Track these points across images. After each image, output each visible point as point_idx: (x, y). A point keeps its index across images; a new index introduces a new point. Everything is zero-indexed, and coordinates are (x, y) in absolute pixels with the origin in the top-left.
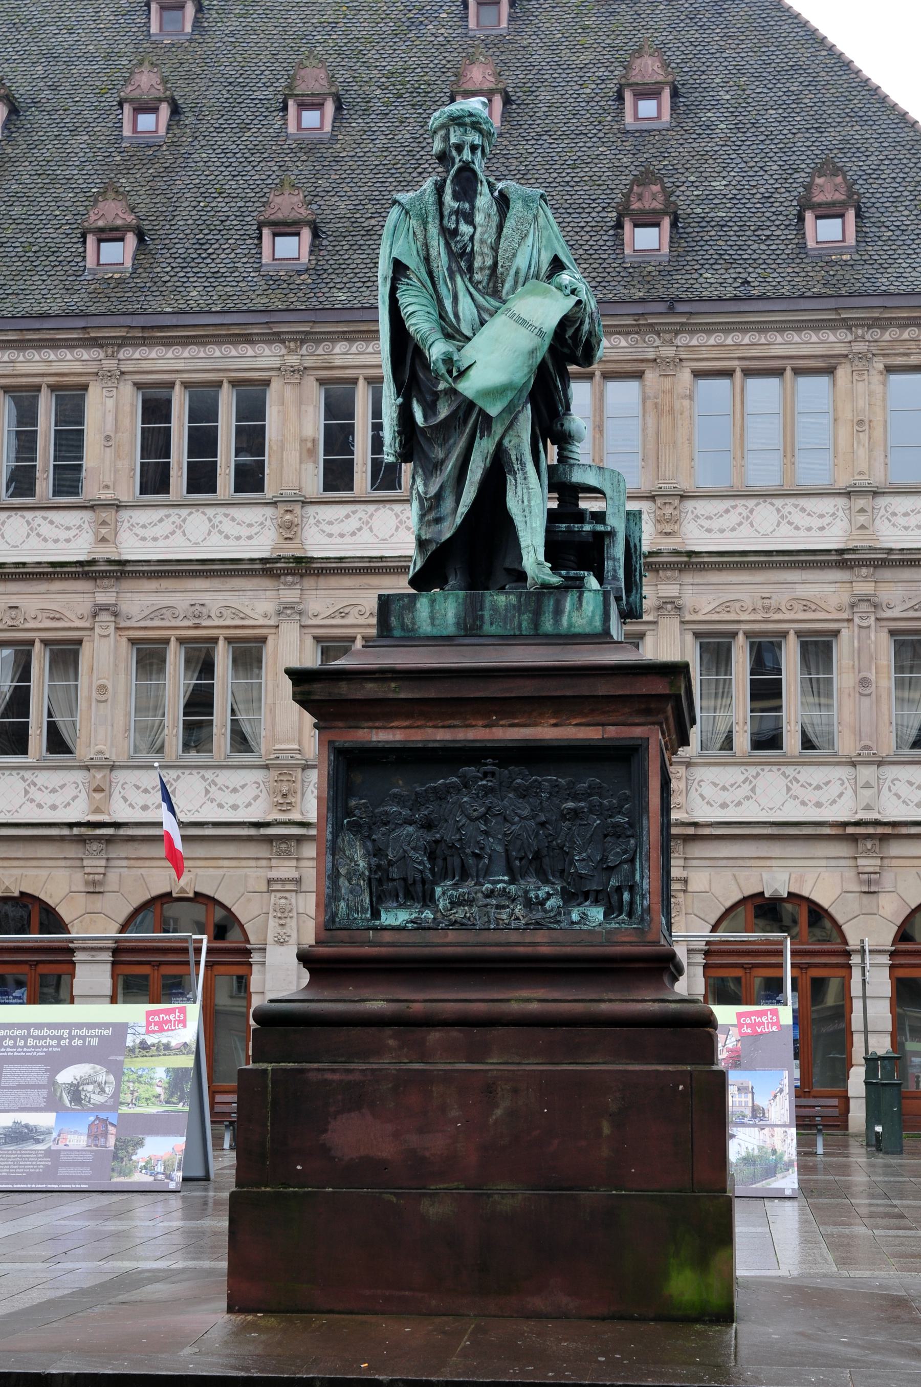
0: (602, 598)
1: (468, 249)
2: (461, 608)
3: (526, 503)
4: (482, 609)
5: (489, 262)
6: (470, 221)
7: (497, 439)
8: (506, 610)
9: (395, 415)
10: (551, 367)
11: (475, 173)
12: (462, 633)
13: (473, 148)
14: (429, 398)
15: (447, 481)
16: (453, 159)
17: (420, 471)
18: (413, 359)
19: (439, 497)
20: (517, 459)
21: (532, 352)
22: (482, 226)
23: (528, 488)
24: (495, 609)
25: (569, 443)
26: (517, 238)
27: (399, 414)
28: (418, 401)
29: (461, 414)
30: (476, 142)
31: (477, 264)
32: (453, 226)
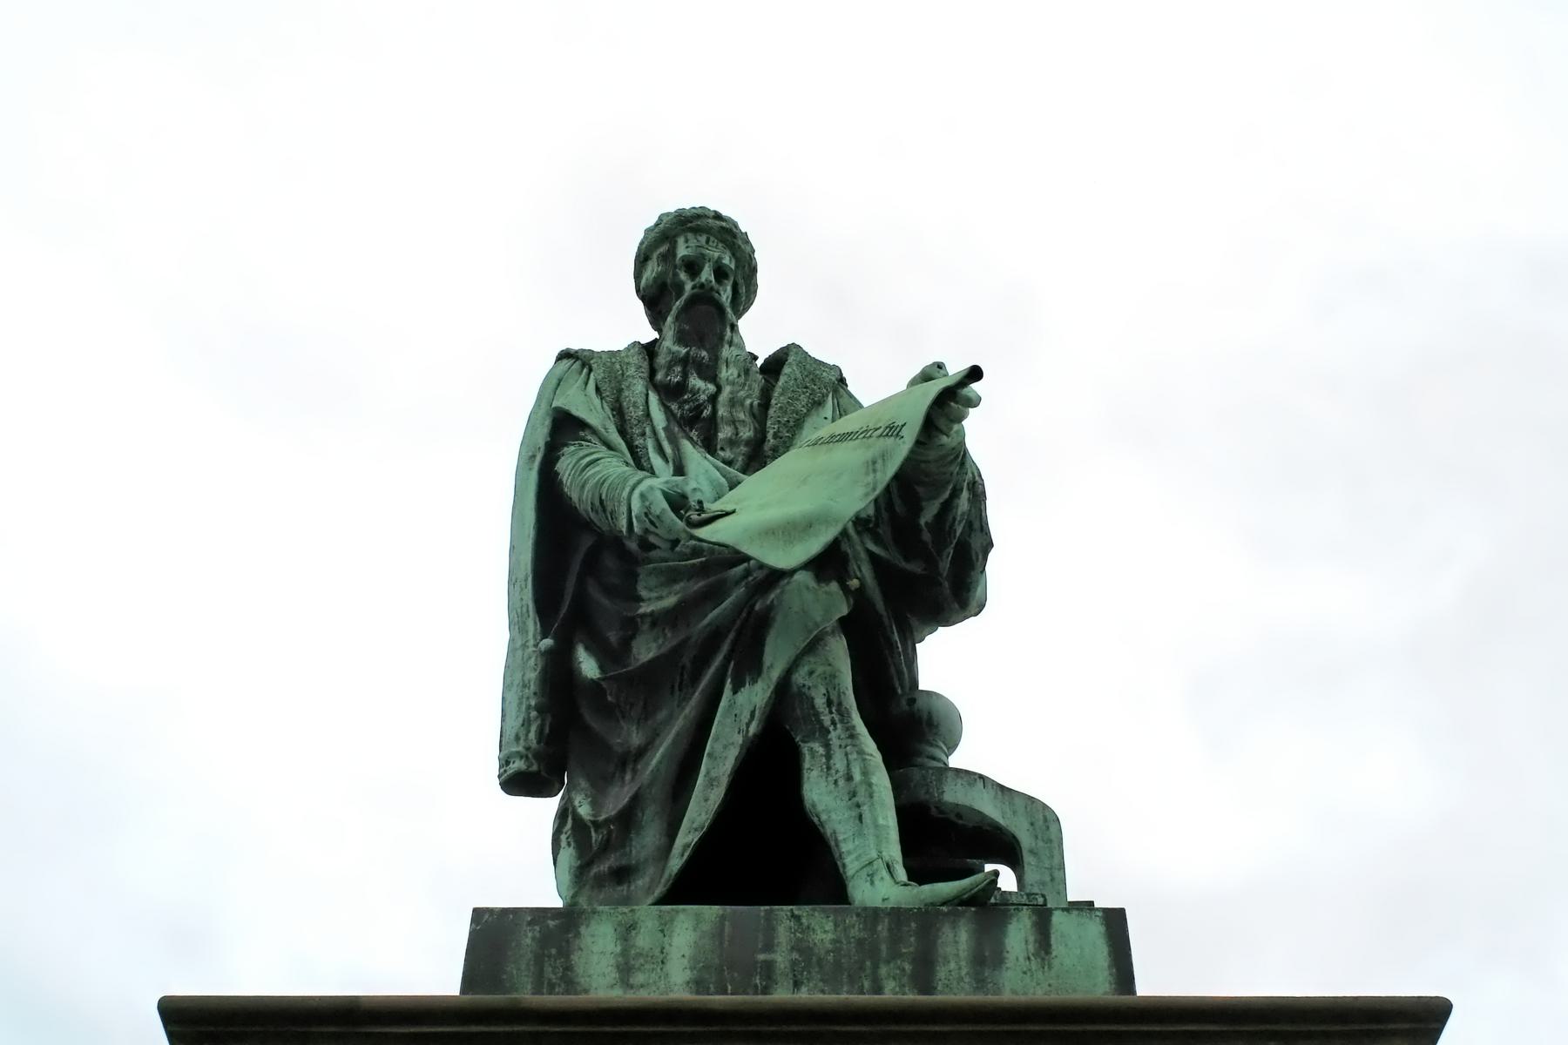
0: (1102, 929)
1: (706, 413)
3: (857, 777)
4: (769, 947)
5: (747, 433)
6: (712, 378)
7: (776, 674)
8: (837, 951)
9: (532, 675)
10: (880, 606)
11: (720, 309)
13: (721, 273)
14: (613, 637)
15: (651, 784)
16: (679, 288)
17: (583, 784)
18: (581, 582)
19: (627, 820)
20: (829, 703)
22: (733, 384)
23: (861, 752)
24: (802, 949)
26: (804, 399)
28: (587, 649)
29: (686, 661)
30: (726, 261)
31: (725, 433)
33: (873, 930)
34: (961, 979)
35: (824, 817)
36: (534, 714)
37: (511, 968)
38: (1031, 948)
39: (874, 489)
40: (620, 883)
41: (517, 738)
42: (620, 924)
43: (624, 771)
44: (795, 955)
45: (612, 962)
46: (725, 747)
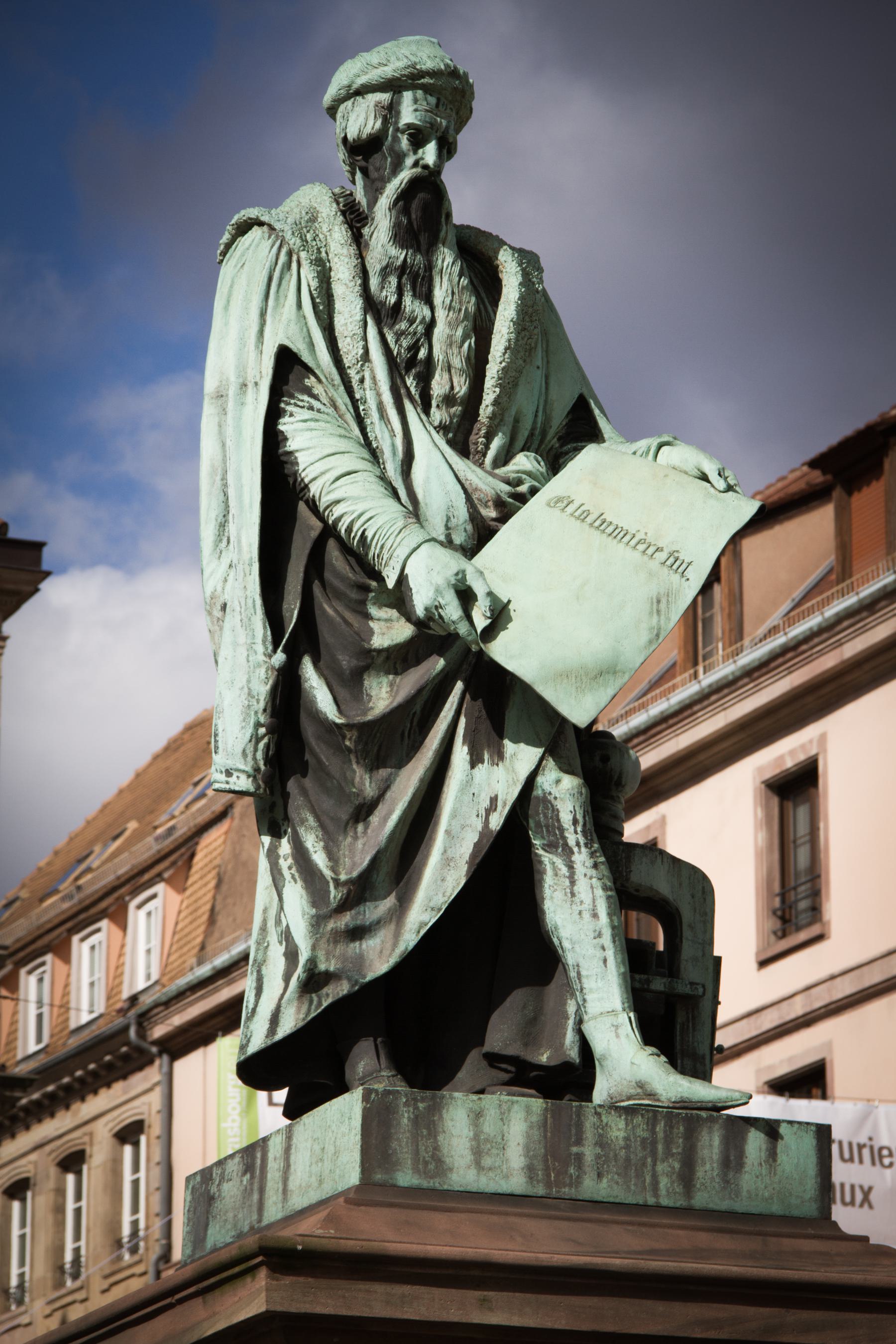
1: (422, 354)
2: (536, 1134)
4: (579, 1141)
5: (462, 388)
7: (523, 770)
8: (627, 1147)
12: (540, 1190)
21: (658, 603)
24: (602, 1142)
25: (612, 798)
29: (418, 708)
31: (439, 386)
32: (393, 299)
33: (653, 1132)
34: (713, 1178)
35: (566, 944)
37: (394, 1145)
38: (763, 1154)
39: (658, 635)
42: (471, 1110)
44: (598, 1150)
45: (468, 1145)
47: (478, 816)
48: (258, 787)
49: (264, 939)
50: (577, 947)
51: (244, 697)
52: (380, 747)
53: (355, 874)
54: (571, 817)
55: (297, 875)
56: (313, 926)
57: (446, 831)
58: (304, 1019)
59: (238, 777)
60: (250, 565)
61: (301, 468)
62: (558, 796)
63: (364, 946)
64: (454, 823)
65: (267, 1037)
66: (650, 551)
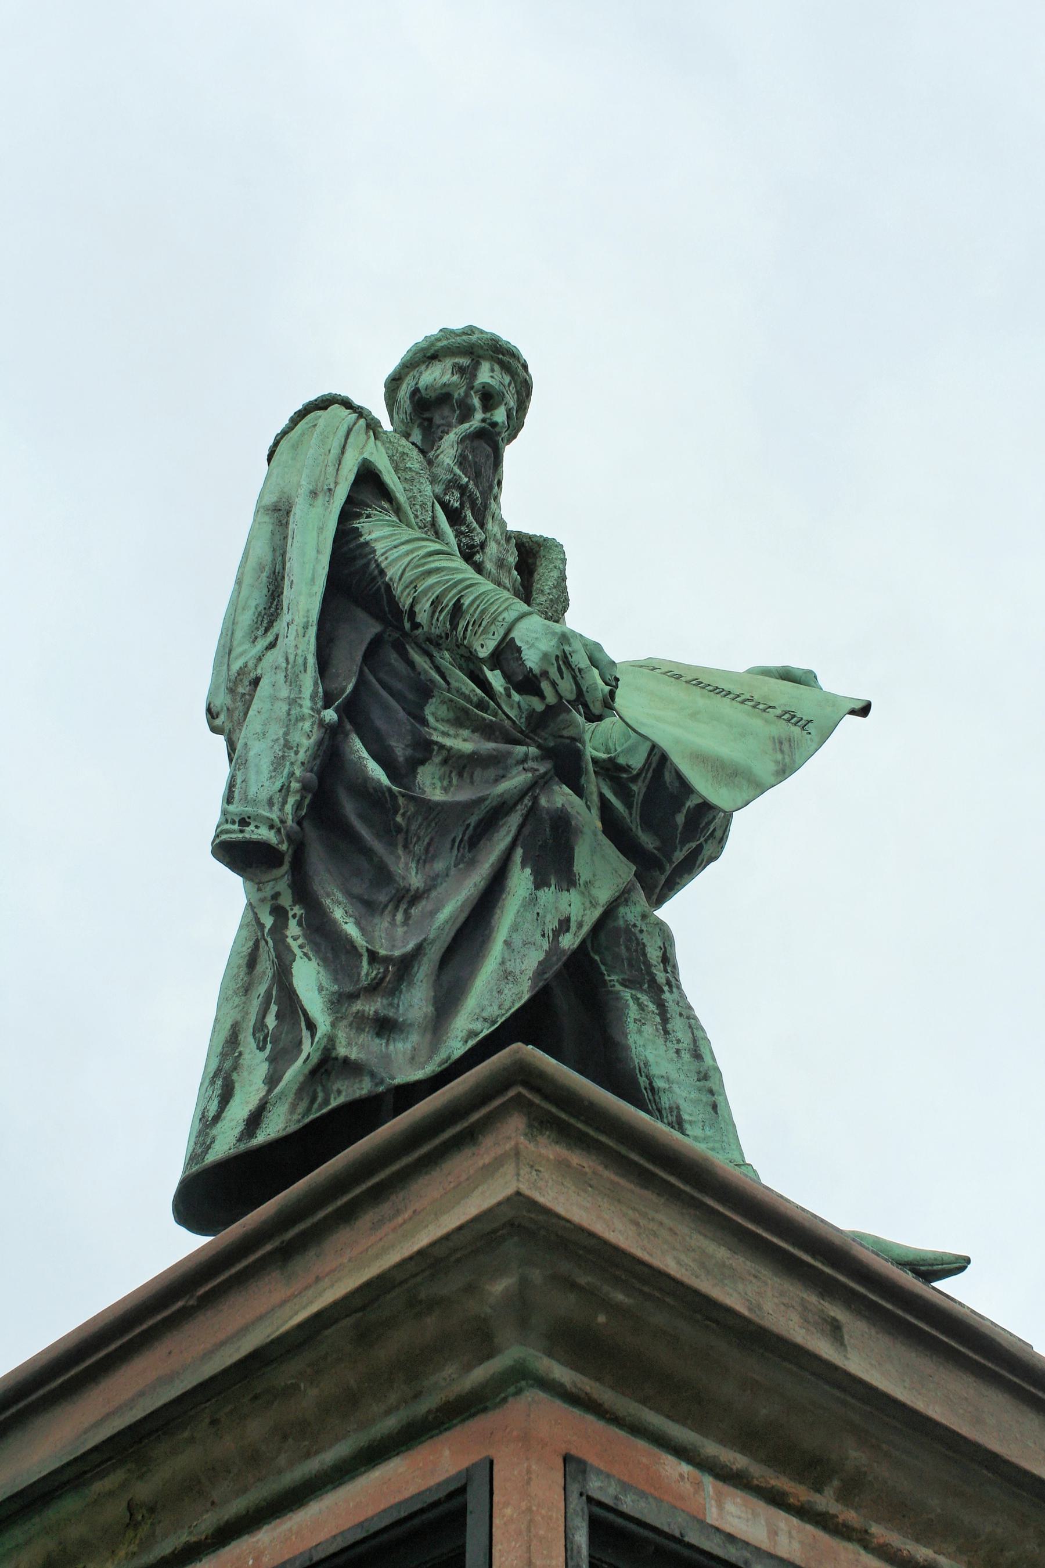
7: (604, 895)
9: (306, 743)
17: (339, 896)
27: (320, 743)
29: (473, 820)
35: (659, 1084)
36: (295, 785)
40: (379, 1035)
41: (270, 803)
43: (397, 908)
46: (525, 944)
47: (543, 935)
48: (281, 842)
49: (234, 1050)
50: (675, 1087)
51: (277, 748)
52: (432, 839)
53: (397, 953)
54: (660, 954)
55: (311, 954)
56: (332, 1003)
57: (505, 941)
58: (299, 1121)
59: (257, 827)
60: (306, 627)
61: (378, 553)
62: (645, 929)
63: (391, 1047)
64: (514, 936)
65: (239, 1140)
66: (761, 706)
